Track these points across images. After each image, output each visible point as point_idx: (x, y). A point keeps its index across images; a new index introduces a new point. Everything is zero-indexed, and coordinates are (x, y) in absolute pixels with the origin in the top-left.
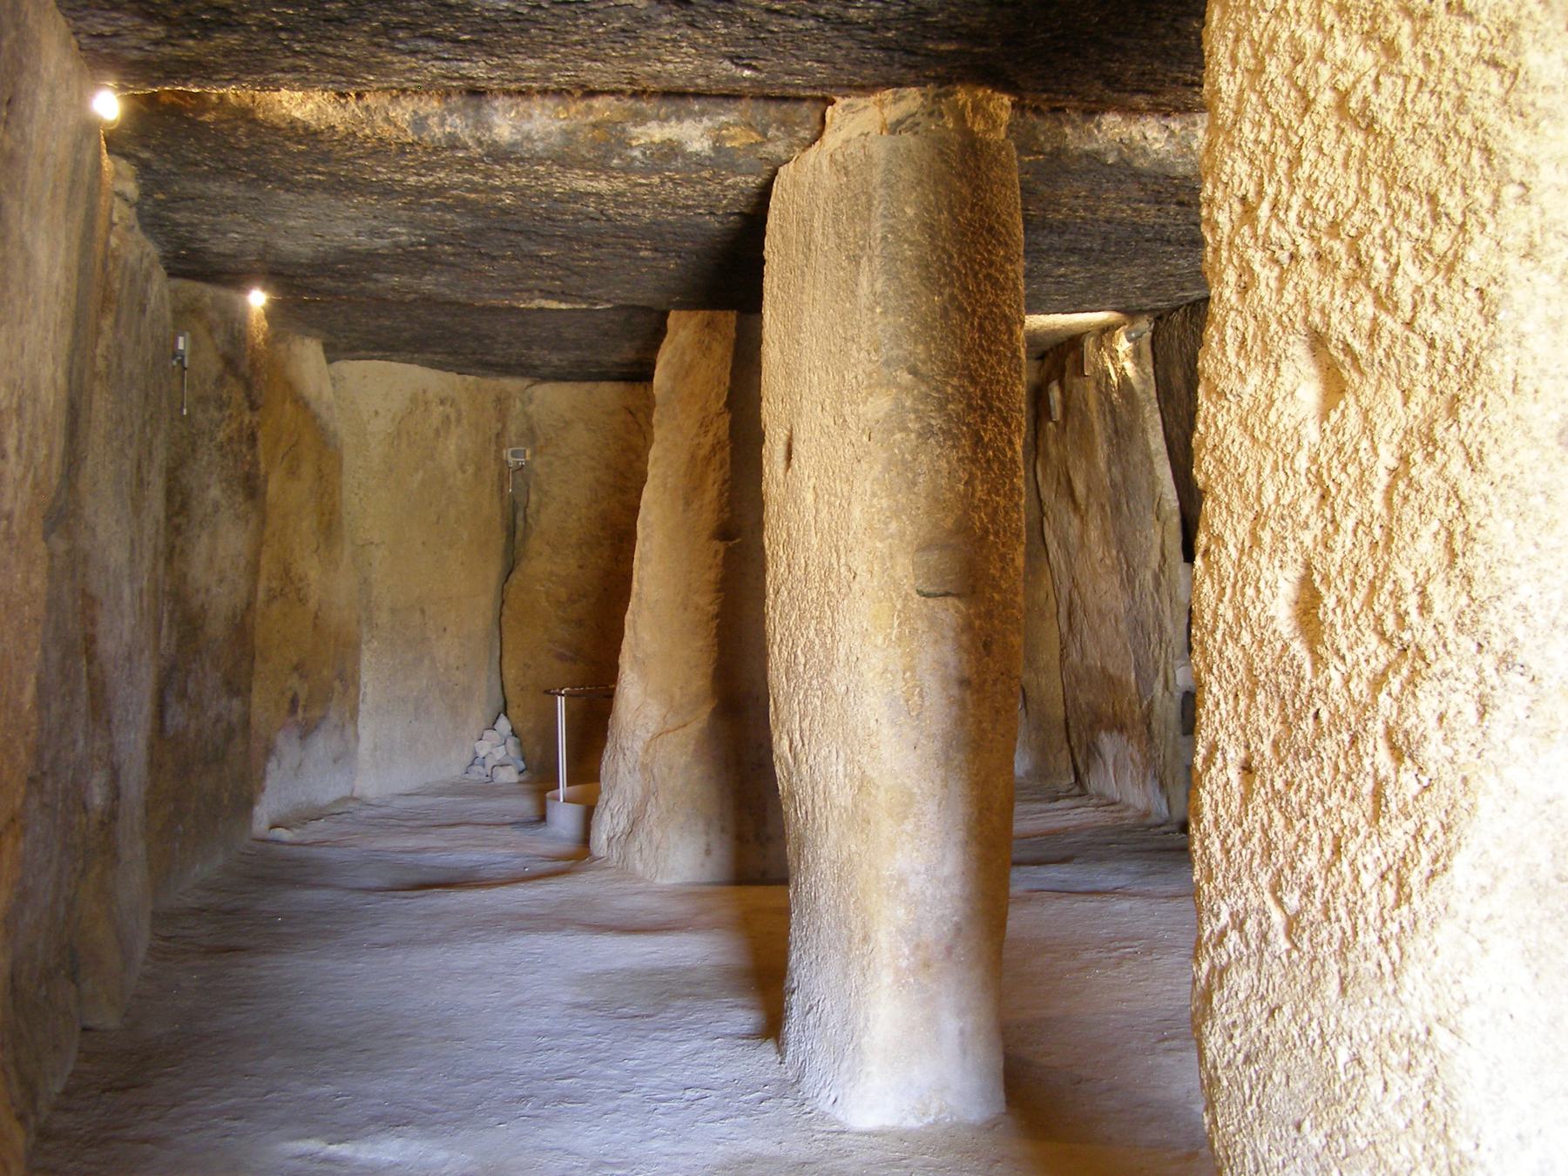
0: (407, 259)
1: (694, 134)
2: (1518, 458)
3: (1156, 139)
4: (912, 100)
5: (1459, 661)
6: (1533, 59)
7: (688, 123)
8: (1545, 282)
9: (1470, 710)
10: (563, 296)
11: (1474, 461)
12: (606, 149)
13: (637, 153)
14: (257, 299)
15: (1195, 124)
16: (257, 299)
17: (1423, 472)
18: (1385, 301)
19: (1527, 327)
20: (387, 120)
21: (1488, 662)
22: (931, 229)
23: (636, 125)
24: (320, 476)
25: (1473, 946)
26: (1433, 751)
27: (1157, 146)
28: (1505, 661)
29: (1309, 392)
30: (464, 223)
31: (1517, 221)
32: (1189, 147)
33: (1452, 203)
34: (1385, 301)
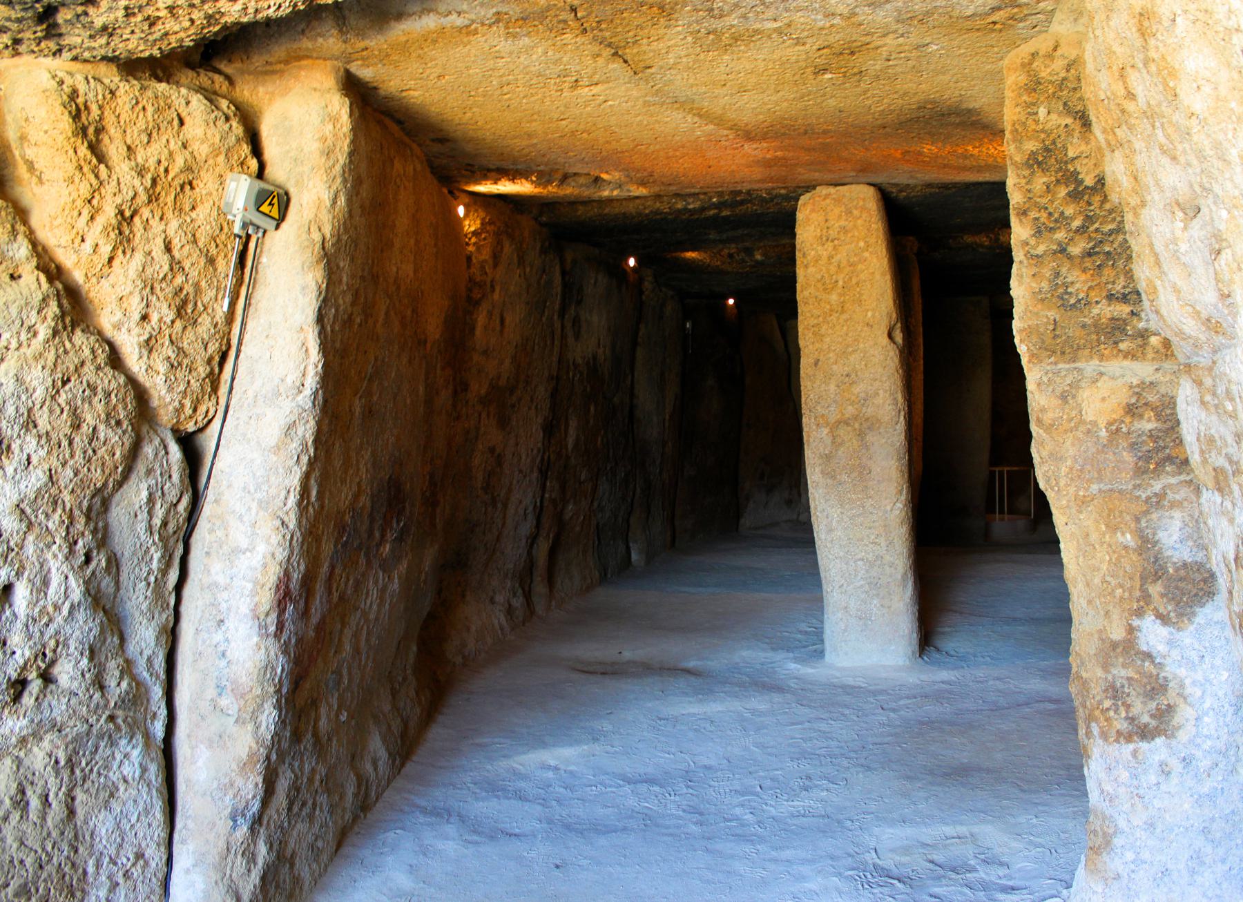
14: (731, 301)
16: (731, 301)
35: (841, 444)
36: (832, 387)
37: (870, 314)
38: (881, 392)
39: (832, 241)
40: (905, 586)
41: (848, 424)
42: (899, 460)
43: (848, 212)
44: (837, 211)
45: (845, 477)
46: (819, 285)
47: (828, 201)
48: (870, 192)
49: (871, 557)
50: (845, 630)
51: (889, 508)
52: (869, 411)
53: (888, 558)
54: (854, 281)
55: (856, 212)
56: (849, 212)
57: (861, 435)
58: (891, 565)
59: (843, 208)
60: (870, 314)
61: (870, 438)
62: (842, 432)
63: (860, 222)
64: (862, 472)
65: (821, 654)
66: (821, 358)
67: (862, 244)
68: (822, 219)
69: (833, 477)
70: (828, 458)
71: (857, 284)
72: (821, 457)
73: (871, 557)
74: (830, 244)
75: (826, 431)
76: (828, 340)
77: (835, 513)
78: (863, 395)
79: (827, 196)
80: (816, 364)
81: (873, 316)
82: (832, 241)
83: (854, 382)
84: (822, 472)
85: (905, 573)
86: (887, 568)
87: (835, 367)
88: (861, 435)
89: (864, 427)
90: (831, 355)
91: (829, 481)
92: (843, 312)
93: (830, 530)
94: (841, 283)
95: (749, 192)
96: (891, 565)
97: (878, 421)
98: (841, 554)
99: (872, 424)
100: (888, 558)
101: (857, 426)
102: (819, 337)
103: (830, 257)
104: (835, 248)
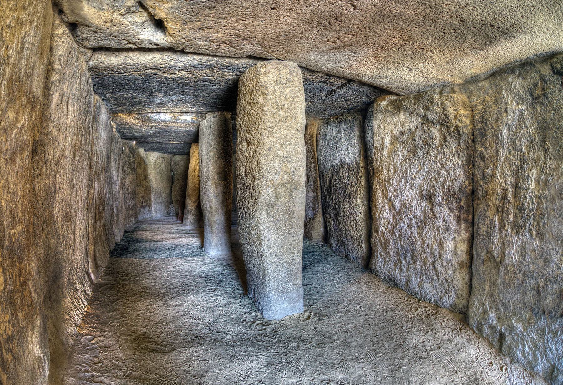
0: (154, 135)
1: (189, 118)
4: (216, 114)
5: (259, 177)
8: (267, 132)
10: (175, 141)
11: (260, 153)
14: (134, 142)
16: (134, 142)
17: (255, 155)
18: (252, 135)
22: (219, 130)
24: (144, 169)
26: (256, 188)
28: (263, 177)
29: (246, 146)
30: (159, 130)
31: (264, 126)
33: (257, 124)
34: (252, 135)
36: (277, 164)
37: (299, 125)
41: (284, 186)
46: (274, 105)
57: (290, 192)
60: (299, 125)
61: (295, 194)
66: (272, 146)
70: (271, 206)
71: (295, 108)
72: (268, 205)
75: (271, 190)
76: (276, 136)
78: (293, 169)
80: (269, 149)
81: (300, 126)
83: (289, 162)
84: (267, 213)
87: (279, 152)
88: (290, 192)
90: (277, 145)
91: (272, 220)
92: (286, 122)
93: (270, 248)
94: (286, 106)
101: (289, 187)
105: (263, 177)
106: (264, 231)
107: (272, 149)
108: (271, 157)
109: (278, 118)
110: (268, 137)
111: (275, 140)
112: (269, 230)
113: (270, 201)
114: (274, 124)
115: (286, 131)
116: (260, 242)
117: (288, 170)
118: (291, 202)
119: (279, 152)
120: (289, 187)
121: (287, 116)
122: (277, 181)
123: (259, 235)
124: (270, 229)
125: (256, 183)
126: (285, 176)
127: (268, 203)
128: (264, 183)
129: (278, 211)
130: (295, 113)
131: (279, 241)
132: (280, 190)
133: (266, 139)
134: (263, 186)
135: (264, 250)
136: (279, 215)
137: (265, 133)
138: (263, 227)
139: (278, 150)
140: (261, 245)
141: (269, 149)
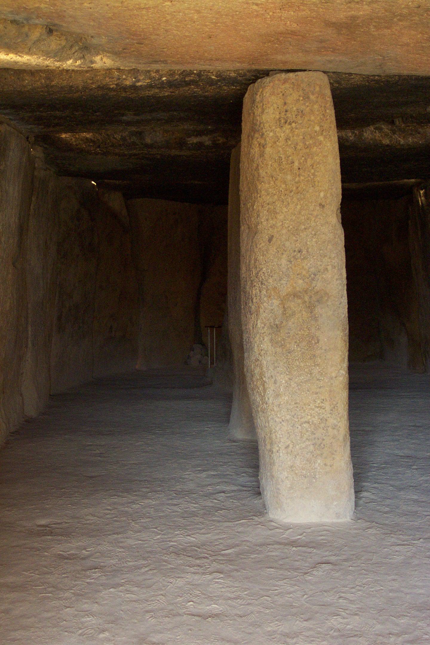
2: (262, 244)
3: (350, 136)
6: (261, 171)
7: (204, 137)
9: (259, 292)
12: (181, 144)
13: (190, 145)
15: (363, 131)
19: (263, 220)
20: (114, 138)
21: (260, 283)
23: (188, 138)
25: (262, 339)
27: (351, 138)
28: (262, 284)
32: (362, 139)
35: (294, 314)
36: (284, 262)
37: (322, 194)
38: (329, 268)
39: (290, 124)
40: (345, 446)
41: (299, 297)
42: (343, 331)
43: (306, 98)
44: (295, 96)
45: (293, 346)
47: (287, 85)
48: (325, 80)
49: (316, 420)
50: (291, 488)
51: (334, 375)
52: (319, 285)
53: (332, 421)
54: (309, 162)
55: (312, 97)
56: (306, 98)
57: (311, 308)
58: (334, 427)
59: (301, 93)
61: (318, 310)
62: (294, 305)
63: (316, 106)
64: (312, 341)
65: (262, 511)
67: (317, 128)
68: (280, 102)
69: (283, 346)
71: (312, 166)
72: (271, 327)
73: (316, 420)
74: (287, 126)
75: (276, 302)
76: (280, 217)
77: (282, 379)
78: (313, 270)
79: (285, 81)
80: (270, 240)
81: (325, 197)
82: (290, 124)
83: (305, 258)
84: (271, 340)
85: (346, 435)
86: (330, 429)
88: (311, 308)
89: (313, 300)
90: (284, 231)
91: (279, 350)
93: (278, 395)
94: (296, 164)
95: (199, 75)
96: (334, 427)
97: (326, 294)
98: (288, 417)
99: (321, 297)
100: (332, 421)
101: (306, 298)
102: (273, 213)
103: (287, 139)
104: (292, 130)
105: (262, 284)
106: (268, 369)
107: (274, 239)
108: (273, 250)
109: (283, 186)
110: (267, 220)
111: (279, 224)
112: (276, 367)
113: (274, 320)
114: (276, 197)
115: (299, 207)
116: (264, 385)
117: (304, 273)
118: (313, 322)
119: (287, 244)
120: (306, 298)
121: (299, 182)
122: (285, 288)
123: (262, 374)
124: (276, 364)
125: (254, 292)
126: (301, 282)
127: (272, 324)
128: (264, 292)
129: (289, 337)
130: (314, 174)
131: (293, 385)
132: (292, 305)
133: (265, 223)
134: (263, 296)
135: (268, 399)
136: (290, 343)
137: (264, 213)
138: (266, 361)
139: (286, 240)
140: (265, 390)
141: (270, 240)
